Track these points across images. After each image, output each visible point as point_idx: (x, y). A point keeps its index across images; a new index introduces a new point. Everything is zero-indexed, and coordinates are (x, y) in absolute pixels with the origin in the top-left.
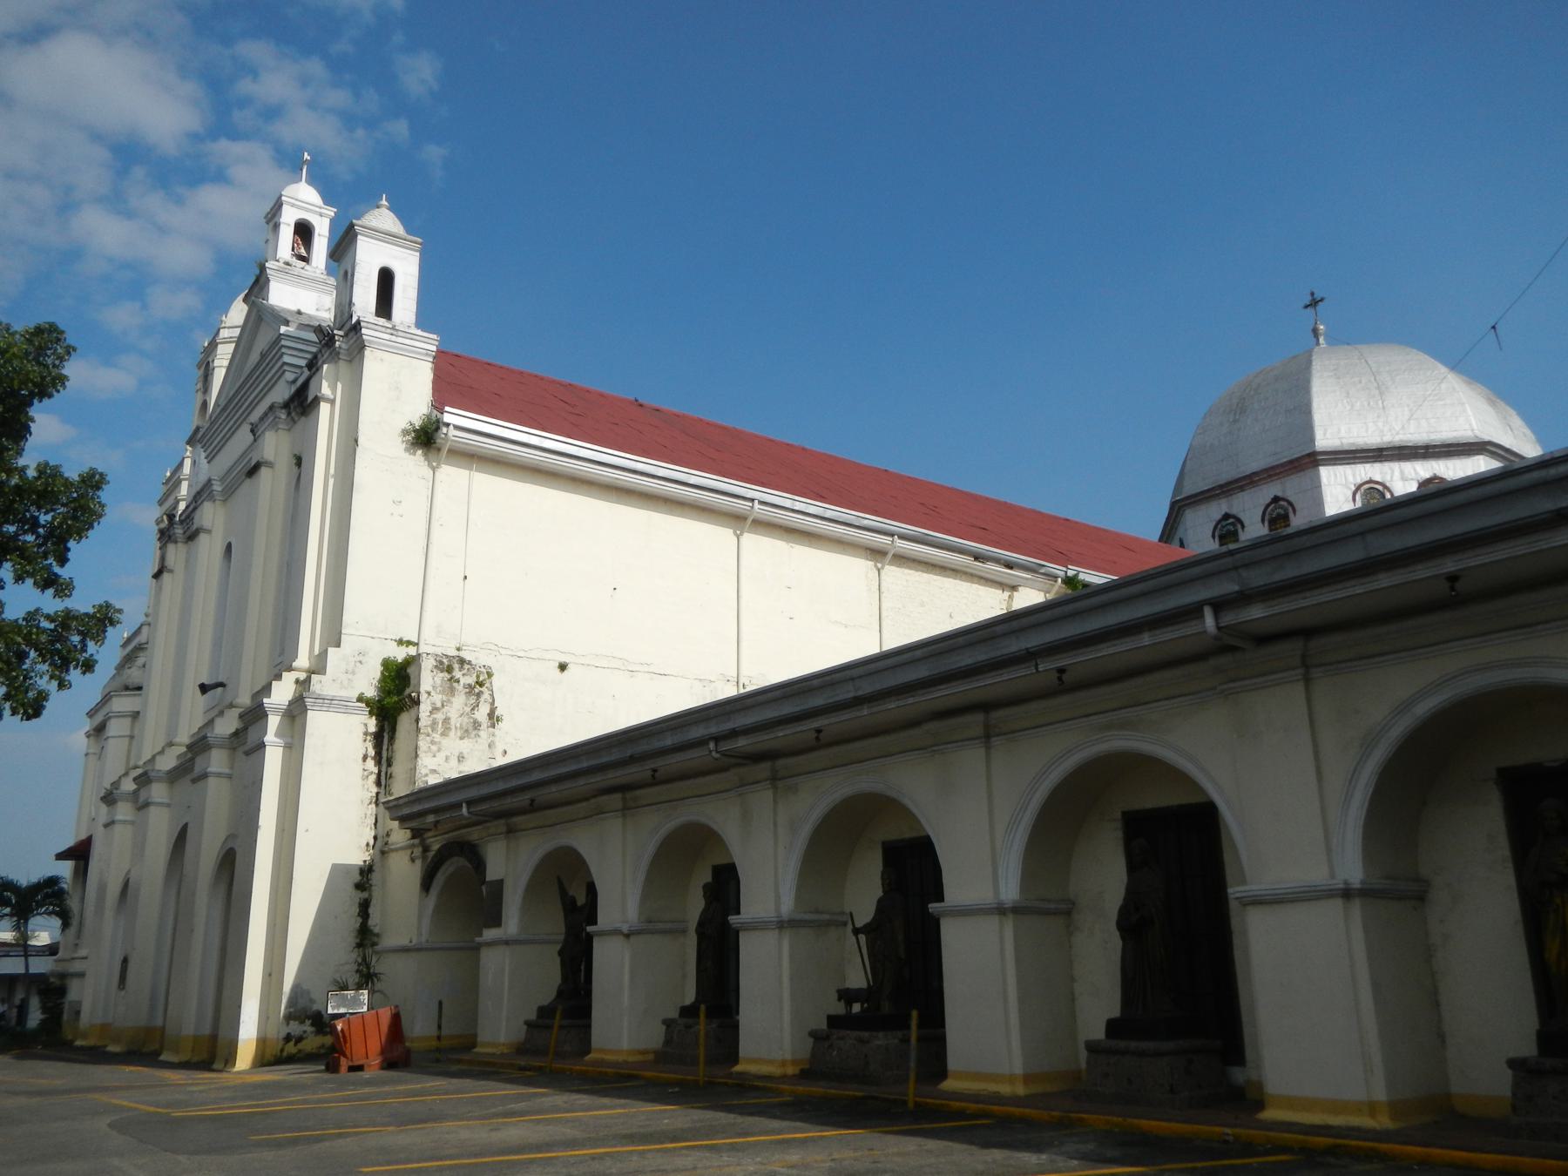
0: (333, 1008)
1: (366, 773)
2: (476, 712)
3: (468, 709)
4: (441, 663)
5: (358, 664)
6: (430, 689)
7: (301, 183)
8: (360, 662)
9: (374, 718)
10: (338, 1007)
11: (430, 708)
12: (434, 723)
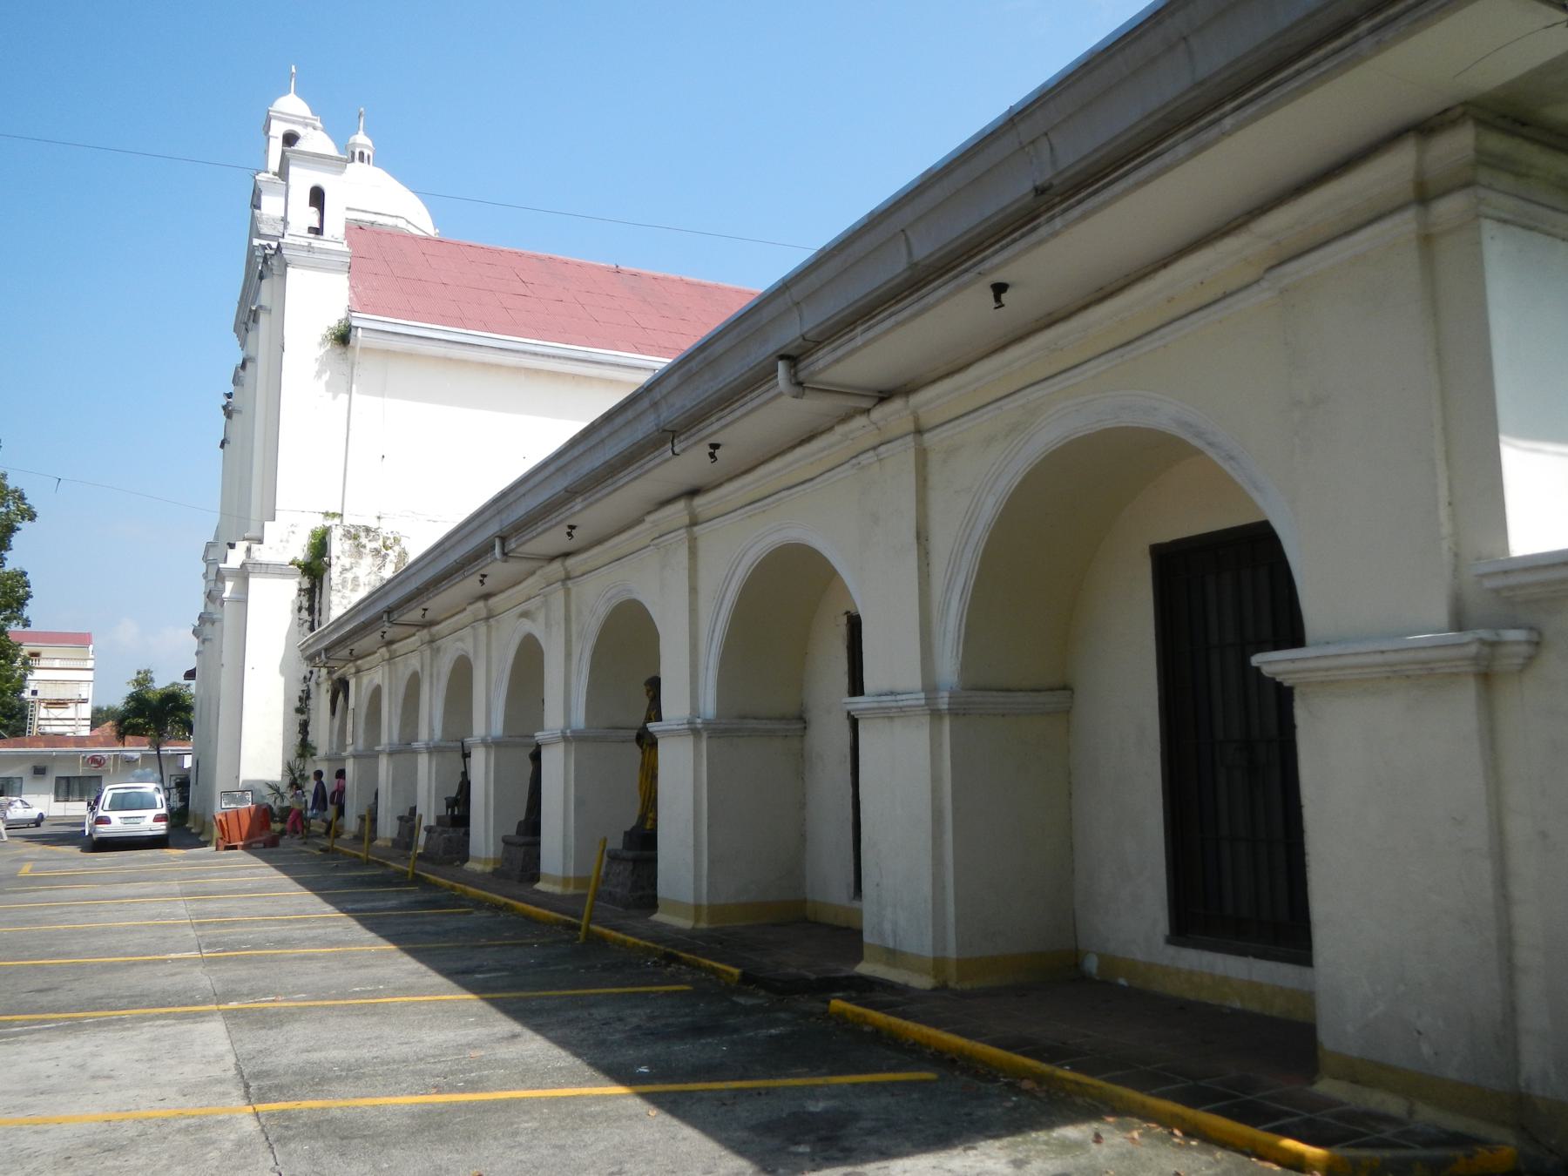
0: (226, 804)
1: (301, 622)
2: (382, 570)
3: (375, 569)
4: (349, 532)
5: (291, 534)
6: (339, 554)
7: (290, 95)
8: (293, 532)
9: (306, 577)
10: (230, 804)
11: (341, 570)
12: (344, 581)
